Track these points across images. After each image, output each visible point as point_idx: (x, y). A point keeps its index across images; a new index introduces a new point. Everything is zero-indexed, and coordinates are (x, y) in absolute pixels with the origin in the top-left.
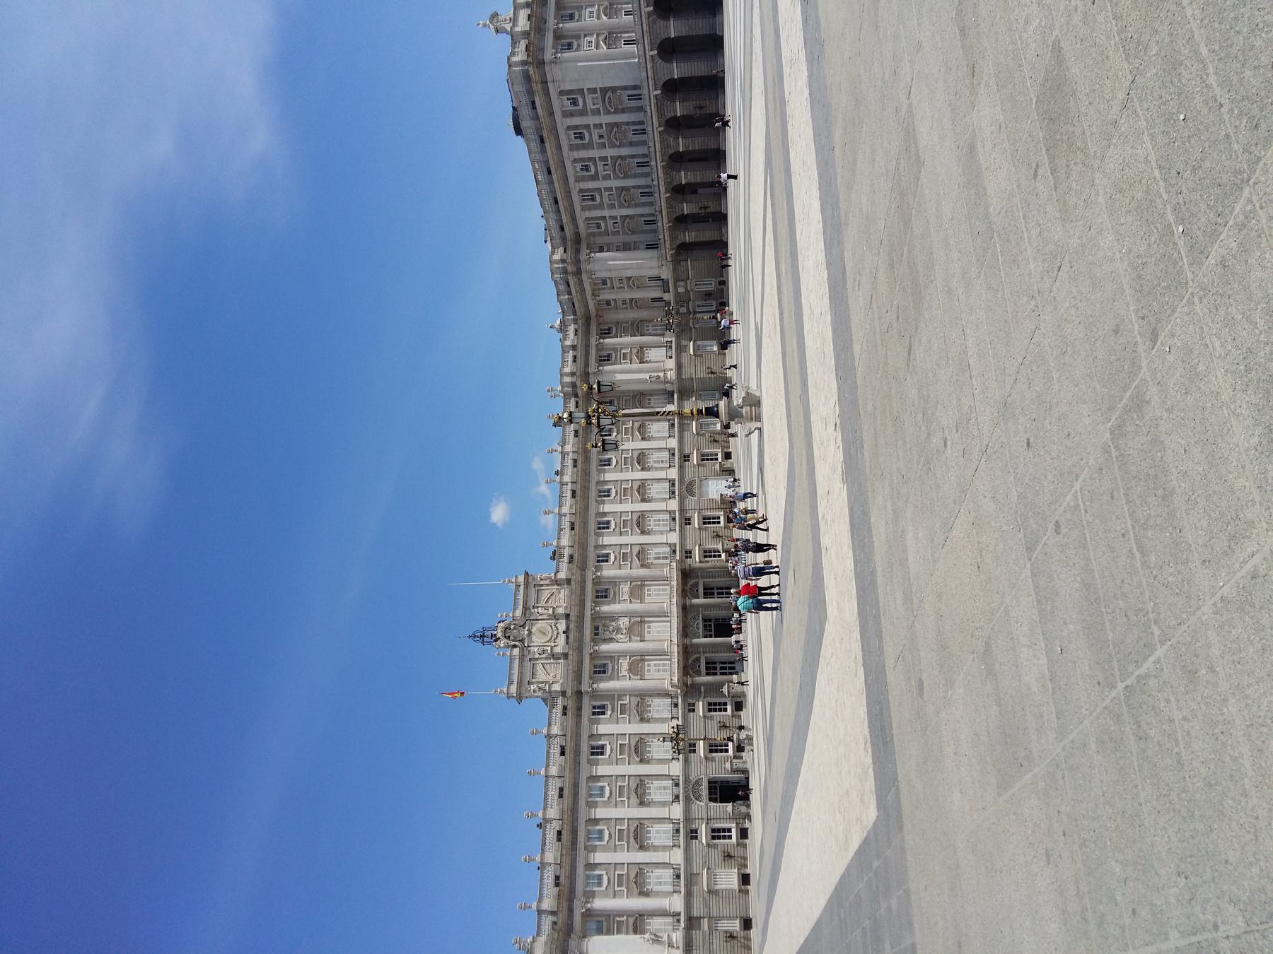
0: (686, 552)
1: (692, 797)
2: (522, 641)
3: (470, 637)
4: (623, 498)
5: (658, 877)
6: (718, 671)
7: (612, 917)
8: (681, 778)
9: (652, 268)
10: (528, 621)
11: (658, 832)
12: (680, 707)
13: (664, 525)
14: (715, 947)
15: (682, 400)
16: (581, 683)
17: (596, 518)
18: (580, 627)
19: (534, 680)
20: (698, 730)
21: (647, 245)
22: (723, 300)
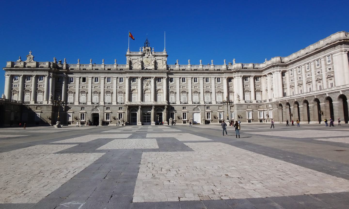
4: (194, 86)
5: (71, 98)
6: (132, 117)
9: (276, 95)
11: (84, 98)
12: (121, 105)
13: (183, 100)
16: (129, 74)
17: (187, 77)
21: (286, 93)
22: (267, 121)
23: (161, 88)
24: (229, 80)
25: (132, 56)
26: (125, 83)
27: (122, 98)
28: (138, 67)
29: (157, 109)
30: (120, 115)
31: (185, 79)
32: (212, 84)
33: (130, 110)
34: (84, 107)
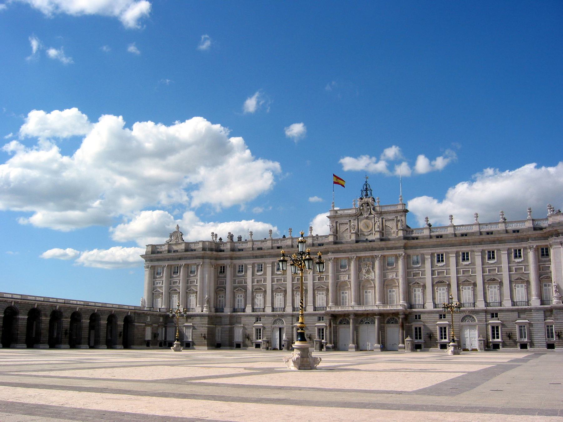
0: (420, 316)
1: (275, 319)
2: (361, 214)
3: (366, 182)
4: (461, 270)
5: (241, 300)
7: (225, 279)
8: (284, 313)
10: (373, 216)
11: (260, 300)
13: (440, 299)
14: (202, 329)
15: (544, 311)
16: (333, 253)
18: (365, 250)
19: (338, 225)
20: (308, 322)
23: (395, 277)
24: (543, 252)
25: (339, 217)
26: (328, 269)
27: (322, 300)
28: (350, 237)
29: (389, 320)
30: (321, 331)
31: (442, 255)
32: (501, 263)
33: (338, 323)
34: (260, 317)
